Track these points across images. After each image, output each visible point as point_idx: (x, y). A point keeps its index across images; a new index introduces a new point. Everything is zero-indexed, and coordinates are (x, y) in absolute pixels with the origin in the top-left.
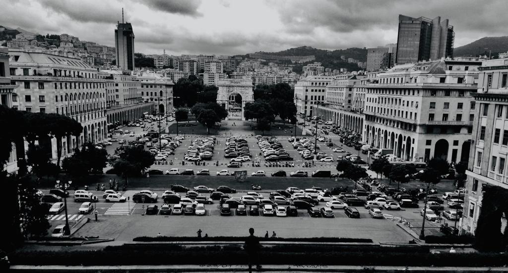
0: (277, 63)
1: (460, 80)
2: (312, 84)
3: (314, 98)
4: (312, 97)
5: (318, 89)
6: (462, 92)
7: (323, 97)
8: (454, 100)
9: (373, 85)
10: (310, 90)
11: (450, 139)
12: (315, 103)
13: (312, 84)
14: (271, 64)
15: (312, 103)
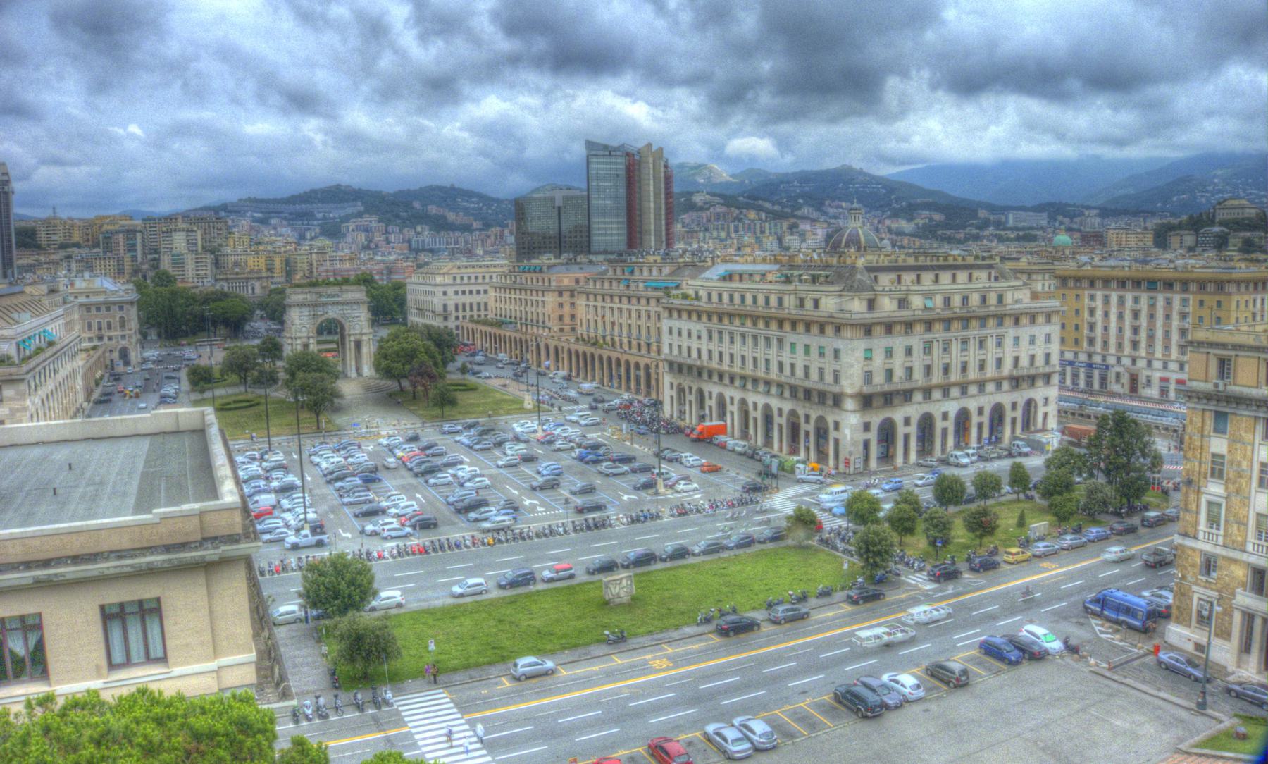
0: (285, 218)
1: (903, 303)
2: (455, 278)
3: (460, 308)
4: (457, 306)
5: (467, 289)
6: (909, 325)
7: (486, 304)
8: (898, 342)
9: (684, 302)
10: (450, 291)
11: (898, 415)
12: (464, 317)
13: (455, 278)
14: (274, 221)
15: (457, 318)
